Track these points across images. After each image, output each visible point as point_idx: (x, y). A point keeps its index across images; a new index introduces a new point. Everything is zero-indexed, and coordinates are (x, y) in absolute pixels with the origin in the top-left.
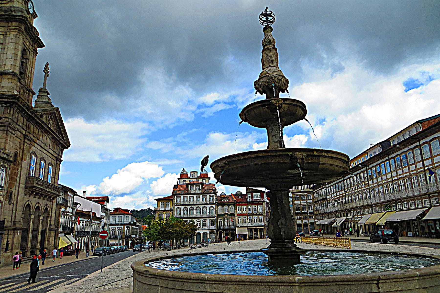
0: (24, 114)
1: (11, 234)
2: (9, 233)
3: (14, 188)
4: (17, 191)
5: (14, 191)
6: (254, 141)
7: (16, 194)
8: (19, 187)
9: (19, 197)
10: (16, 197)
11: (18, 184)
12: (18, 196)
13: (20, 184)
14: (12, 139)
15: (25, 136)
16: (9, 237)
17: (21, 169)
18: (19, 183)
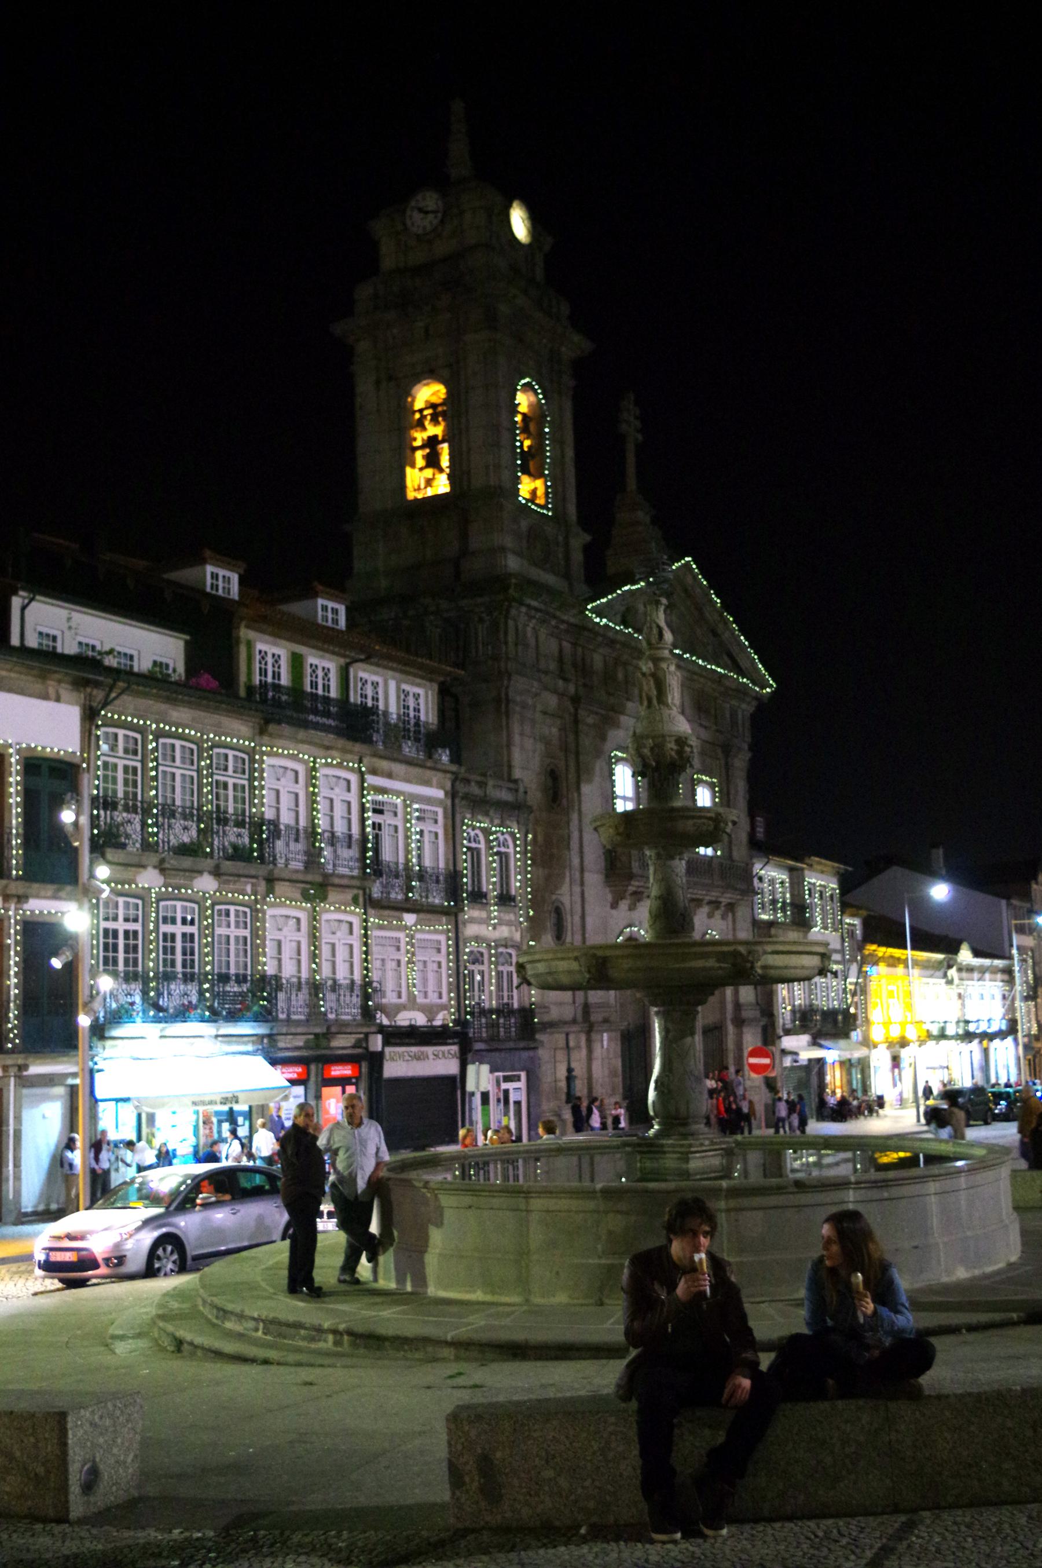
0: (557, 627)
1: (578, 1047)
2: (572, 1044)
3: (565, 889)
4: (577, 898)
5: (566, 900)
6: (608, 908)
7: (578, 908)
8: (582, 884)
9: (589, 920)
10: (577, 919)
11: (577, 875)
12: (583, 917)
13: (587, 875)
14: (527, 729)
15: (576, 700)
16: (572, 1058)
17: (580, 821)
18: (582, 870)
